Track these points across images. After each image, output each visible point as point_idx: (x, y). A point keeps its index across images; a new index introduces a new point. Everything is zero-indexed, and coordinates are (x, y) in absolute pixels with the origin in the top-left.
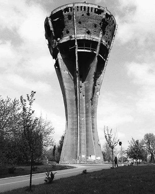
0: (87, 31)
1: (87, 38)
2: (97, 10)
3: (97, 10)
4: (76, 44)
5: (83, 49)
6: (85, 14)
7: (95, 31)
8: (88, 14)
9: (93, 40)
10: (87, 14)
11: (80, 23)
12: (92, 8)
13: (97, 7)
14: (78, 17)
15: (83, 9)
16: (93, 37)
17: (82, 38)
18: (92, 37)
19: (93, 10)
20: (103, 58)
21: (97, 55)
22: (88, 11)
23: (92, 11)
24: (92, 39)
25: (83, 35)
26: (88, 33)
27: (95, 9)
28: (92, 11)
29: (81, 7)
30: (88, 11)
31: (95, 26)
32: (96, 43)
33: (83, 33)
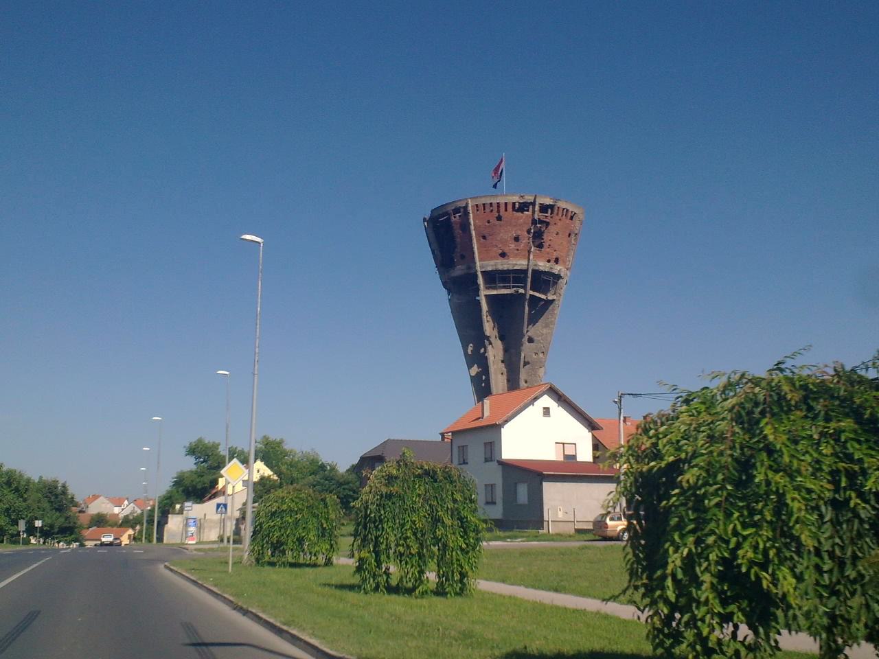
0: (501, 251)
1: (500, 267)
2: (517, 205)
3: (517, 205)
4: (481, 281)
5: (495, 288)
6: (494, 221)
7: (518, 250)
8: (499, 218)
9: (515, 268)
10: (497, 218)
11: (484, 238)
12: (506, 203)
13: (516, 199)
14: (480, 227)
15: (488, 210)
16: (514, 262)
17: (489, 269)
18: (510, 262)
19: (510, 207)
20: (543, 297)
21: (528, 297)
22: (498, 211)
23: (506, 210)
24: (511, 268)
25: (492, 262)
26: (503, 255)
27: (514, 204)
28: (506, 210)
29: (484, 205)
30: (498, 211)
31: (517, 239)
32: (525, 272)
33: (492, 258)
